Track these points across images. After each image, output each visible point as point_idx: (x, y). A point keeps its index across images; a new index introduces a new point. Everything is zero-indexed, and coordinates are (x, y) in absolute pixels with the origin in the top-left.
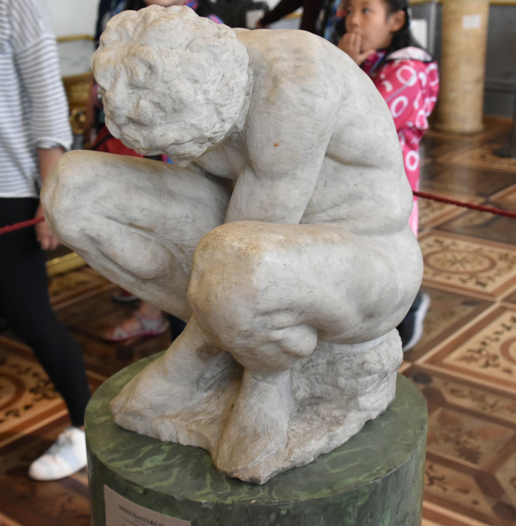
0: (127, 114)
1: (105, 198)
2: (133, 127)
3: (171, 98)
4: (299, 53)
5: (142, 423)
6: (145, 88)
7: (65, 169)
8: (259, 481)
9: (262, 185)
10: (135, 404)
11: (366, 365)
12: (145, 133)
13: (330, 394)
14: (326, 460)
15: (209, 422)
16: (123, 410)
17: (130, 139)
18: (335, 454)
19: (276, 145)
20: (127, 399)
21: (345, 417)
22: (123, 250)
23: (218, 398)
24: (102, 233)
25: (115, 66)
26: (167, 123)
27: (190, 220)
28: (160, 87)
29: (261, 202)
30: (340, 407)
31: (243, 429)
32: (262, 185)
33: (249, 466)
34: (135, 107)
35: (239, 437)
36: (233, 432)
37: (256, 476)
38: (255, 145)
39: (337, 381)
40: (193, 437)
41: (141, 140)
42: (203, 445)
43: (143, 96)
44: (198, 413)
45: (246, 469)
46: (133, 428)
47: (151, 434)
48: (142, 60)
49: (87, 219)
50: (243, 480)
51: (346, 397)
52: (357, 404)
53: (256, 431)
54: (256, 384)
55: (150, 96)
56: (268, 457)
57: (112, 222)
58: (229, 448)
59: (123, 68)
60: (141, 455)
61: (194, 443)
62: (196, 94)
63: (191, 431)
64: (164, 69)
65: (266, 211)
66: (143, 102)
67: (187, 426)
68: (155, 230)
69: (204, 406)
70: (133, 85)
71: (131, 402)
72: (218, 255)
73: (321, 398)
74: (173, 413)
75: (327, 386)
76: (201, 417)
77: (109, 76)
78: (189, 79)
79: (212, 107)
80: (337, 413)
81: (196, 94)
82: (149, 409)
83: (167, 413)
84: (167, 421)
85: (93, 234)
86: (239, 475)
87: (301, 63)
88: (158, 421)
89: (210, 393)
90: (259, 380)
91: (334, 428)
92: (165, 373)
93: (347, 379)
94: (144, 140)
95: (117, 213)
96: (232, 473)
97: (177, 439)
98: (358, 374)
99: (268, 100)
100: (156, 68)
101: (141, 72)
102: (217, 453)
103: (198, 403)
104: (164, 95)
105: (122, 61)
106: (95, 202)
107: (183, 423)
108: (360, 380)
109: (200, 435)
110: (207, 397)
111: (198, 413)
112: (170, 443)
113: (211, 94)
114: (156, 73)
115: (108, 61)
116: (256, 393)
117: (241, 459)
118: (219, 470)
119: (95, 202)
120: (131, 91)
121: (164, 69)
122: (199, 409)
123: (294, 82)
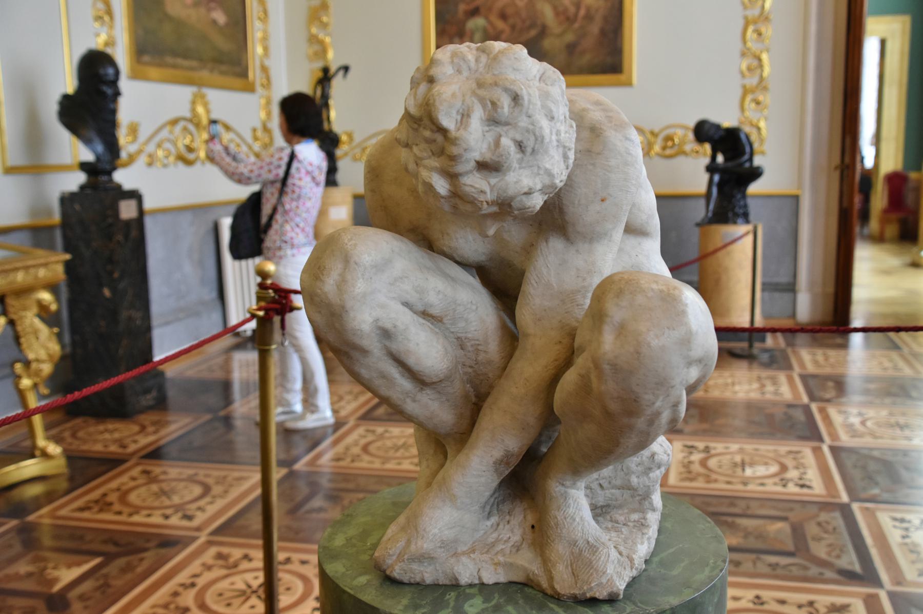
0: (478, 158)
1: (401, 278)
2: (478, 175)
3: (535, 135)
4: (601, 105)
5: (430, 569)
6: (507, 124)
7: (355, 245)
8: (619, 595)
9: (577, 251)
10: (426, 545)
11: (656, 457)
12: (493, 181)
13: (616, 500)
14: (654, 566)
15: (514, 550)
16: (406, 557)
17: (473, 190)
18: (656, 559)
19: (603, 200)
20: (409, 542)
21: (645, 518)
22: (418, 344)
23: (508, 522)
24: (399, 324)
25: (463, 101)
26: (520, 168)
27: (474, 307)
28: (523, 122)
29: (578, 270)
30: (634, 511)
31: (574, 543)
32: (577, 251)
33: (604, 581)
34: (493, 147)
35: (573, 553)
36: (559, 550)
37: (615, 589)
39: (629, 481)
40: (500, 570)
41: (488, 191)
42: (518, 577)
43: (502, 133)
44: (493, 545)
45: (600, 585)
46: (418, 579)
47: (443, 581)
48: (506, 90)
49: (382, 306)
50: (601, 598)
51: (637, 498)
52: (651, 504)
53: (588, 542)
54: (566, 492)
55: (512, 133)
56: (615, 568)
57: (406, 310)
58: (567, 567)
59: (476, 101)
60: (452, 604)
61: (502, 579)
62: (551, 134)
63: (497, 564)
64: (529, 101)
65: (584, 279)
66: (506, 142)
67: (492, 559)
68: (445, 321)
69: (495, 535)
70: (493, 121)
71: (416, 544)
72: (640, 299)
73: (608, 506)
74: (465, 549)
75: (613, 491)
76: (500, 547)
77: (454, 112)
78: (546, 116)
79: (561, 150)
80: (635, 516)
81: (551, 134)
82: (441, 547)
83: (459, 550)
84: (464, 559)
85: (388, 325)
87: (610, 114)
88: (452, 560)
89: (494, 519)
90: (568, 487)
91: (645, 531)
92: (453, 499)
93: (638, 477)
94: (491, 190)
95: (413, 298)
96: (584, 594)
97: (480, 578)
98: (650, 469)
99: (589, 151)
100: (523, 99)
101: (505, 102)
102: (551, 578)
103: (485, 533)
104: (528, 131)
105: (474, 93)
106: (391, 284)
107: (486, 557)
108: (651, 475)
109: (509, 566)
110: (492, 526)
111: (493, 545)
112: (471, 586)
113: (563, 135)
114: (522, 105)
115: (453, 95)
116: (571, 501)
117: (592, 574)
118: (564, 595)
119: (391, 284)
120: (487, 128)
121: (529, 101)
122: (491, 540)
123: (616, 130)
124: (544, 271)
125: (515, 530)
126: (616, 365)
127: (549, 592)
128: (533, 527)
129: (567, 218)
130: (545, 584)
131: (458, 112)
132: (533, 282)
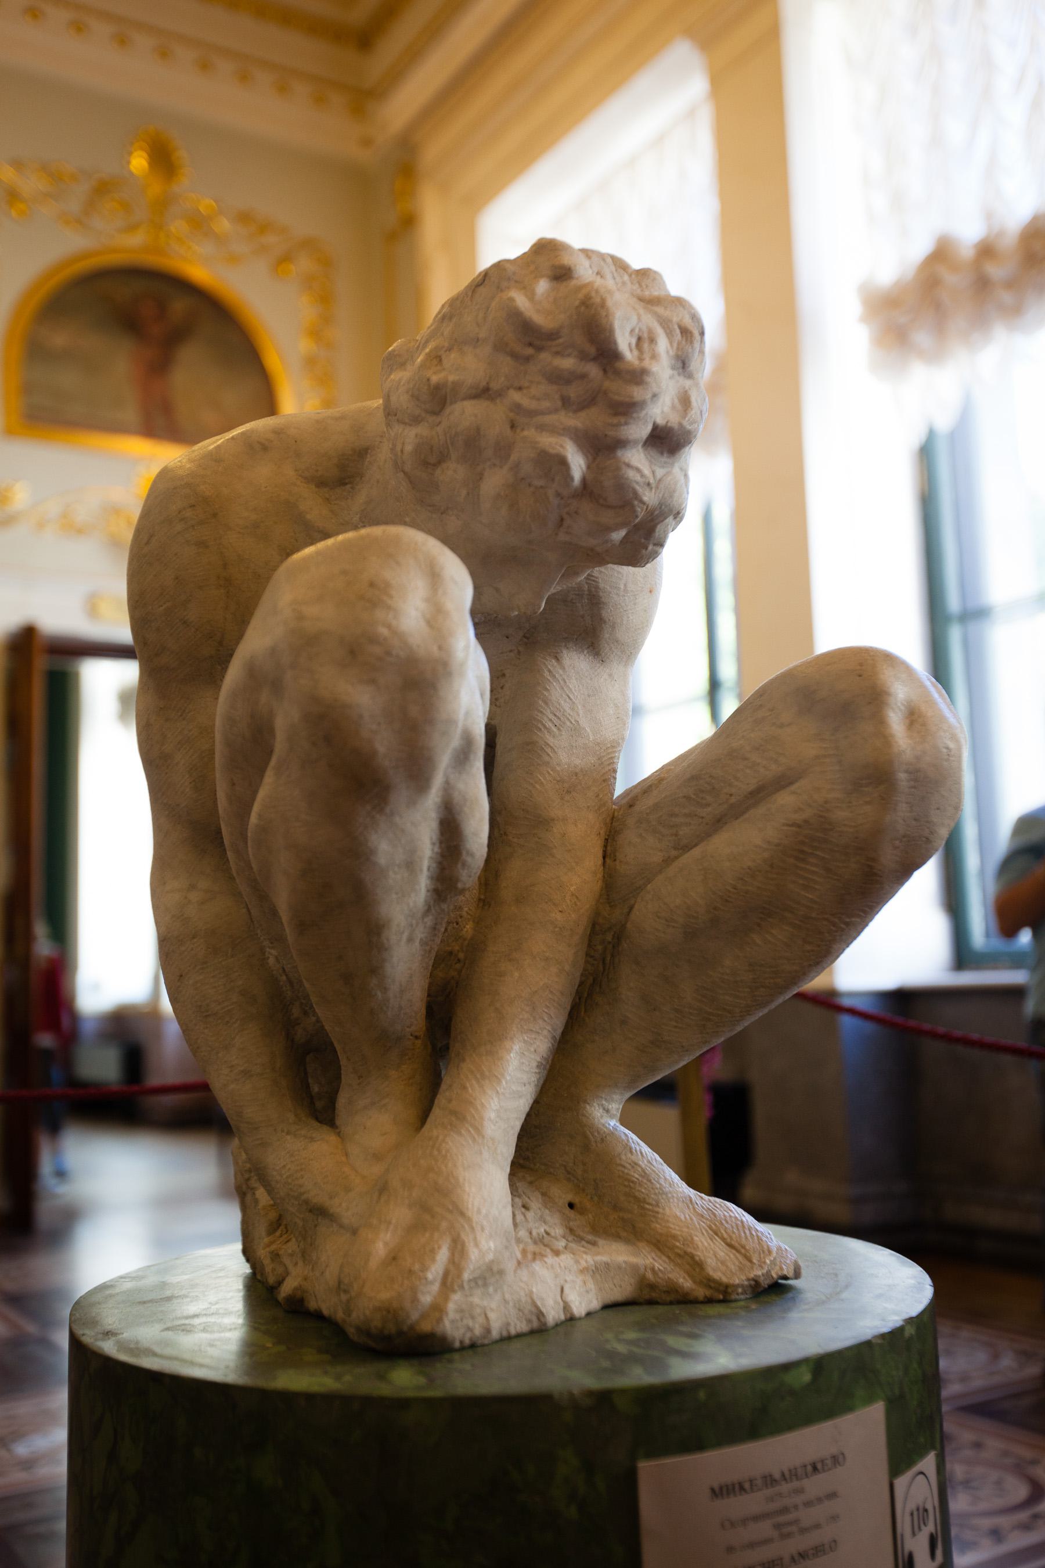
0: (660, 421)
17: (638, 478)
32: (610, 675)
38: (622, 587)
86: (781, 1269)
124: (566, 706)
125: (548, 1218)
126: (918, 771)
127: (701, 1293)
128: (571, 1206)
129: (604, 614)
130: (686, 1283)
131: (632, 331)
132: (549, 724)
